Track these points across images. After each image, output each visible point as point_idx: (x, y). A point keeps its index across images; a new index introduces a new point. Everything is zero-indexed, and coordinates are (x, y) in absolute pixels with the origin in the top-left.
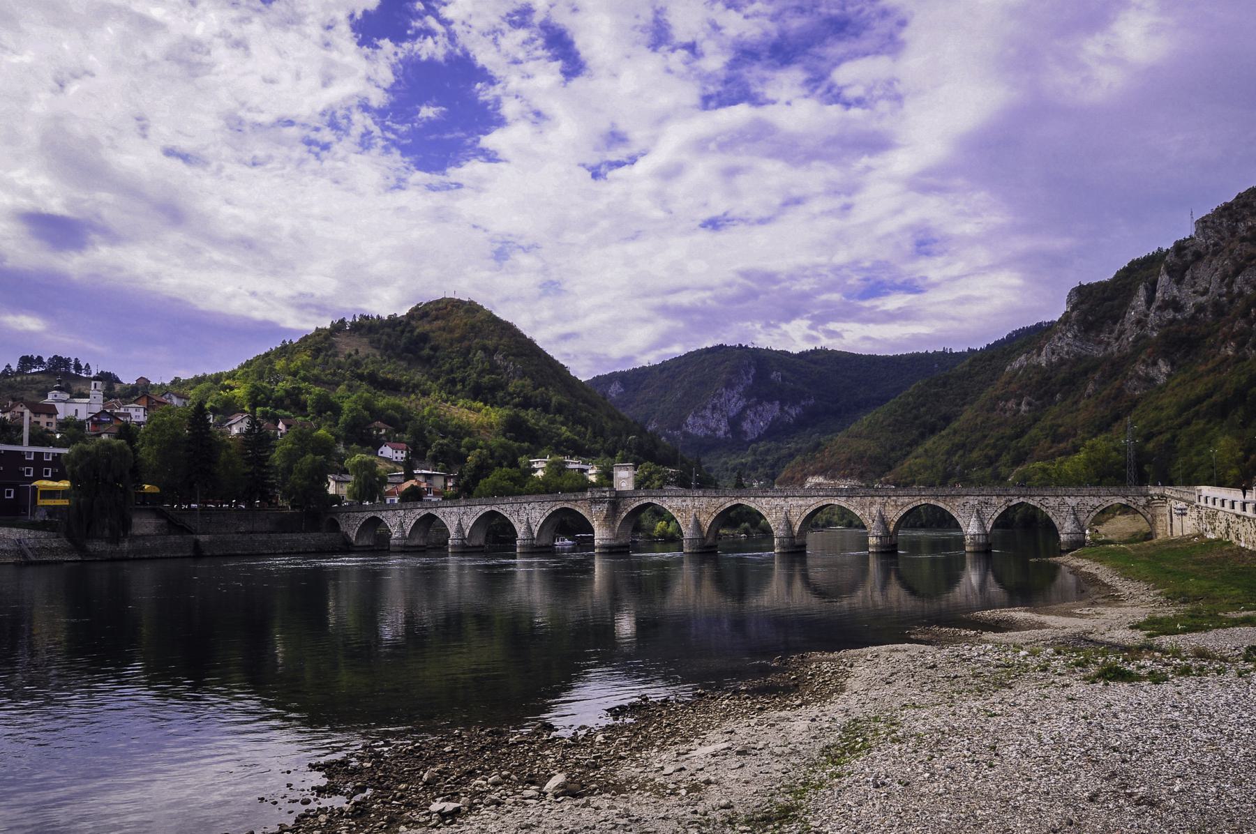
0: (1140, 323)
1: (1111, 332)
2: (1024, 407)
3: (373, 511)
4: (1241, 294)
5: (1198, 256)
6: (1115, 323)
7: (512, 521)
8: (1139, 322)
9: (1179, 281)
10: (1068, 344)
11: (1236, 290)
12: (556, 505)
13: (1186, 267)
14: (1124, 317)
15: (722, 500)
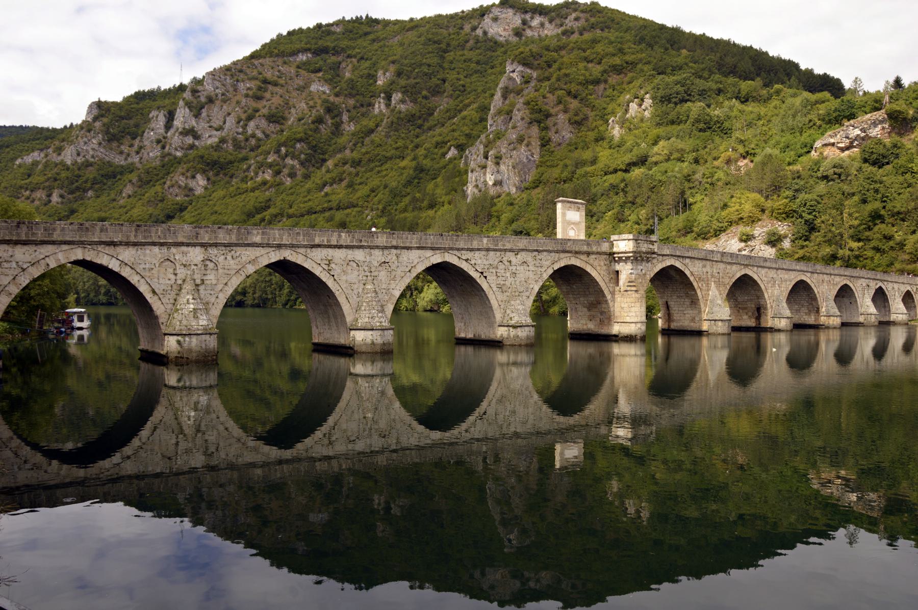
0: (161, 142)
1: (131, 146)
2: (55, 198)
3: (81, 244)
4: (253, 136)
5: (210, 100)
6: (134, 138)
7: (485, 286)
8: (159, 141)
9: (197, 116)
10: (93, 149)
11: (250, 132)
12: (559, 259)
13: (202, 107)
14: (142, 136)
15: (734, 267)
